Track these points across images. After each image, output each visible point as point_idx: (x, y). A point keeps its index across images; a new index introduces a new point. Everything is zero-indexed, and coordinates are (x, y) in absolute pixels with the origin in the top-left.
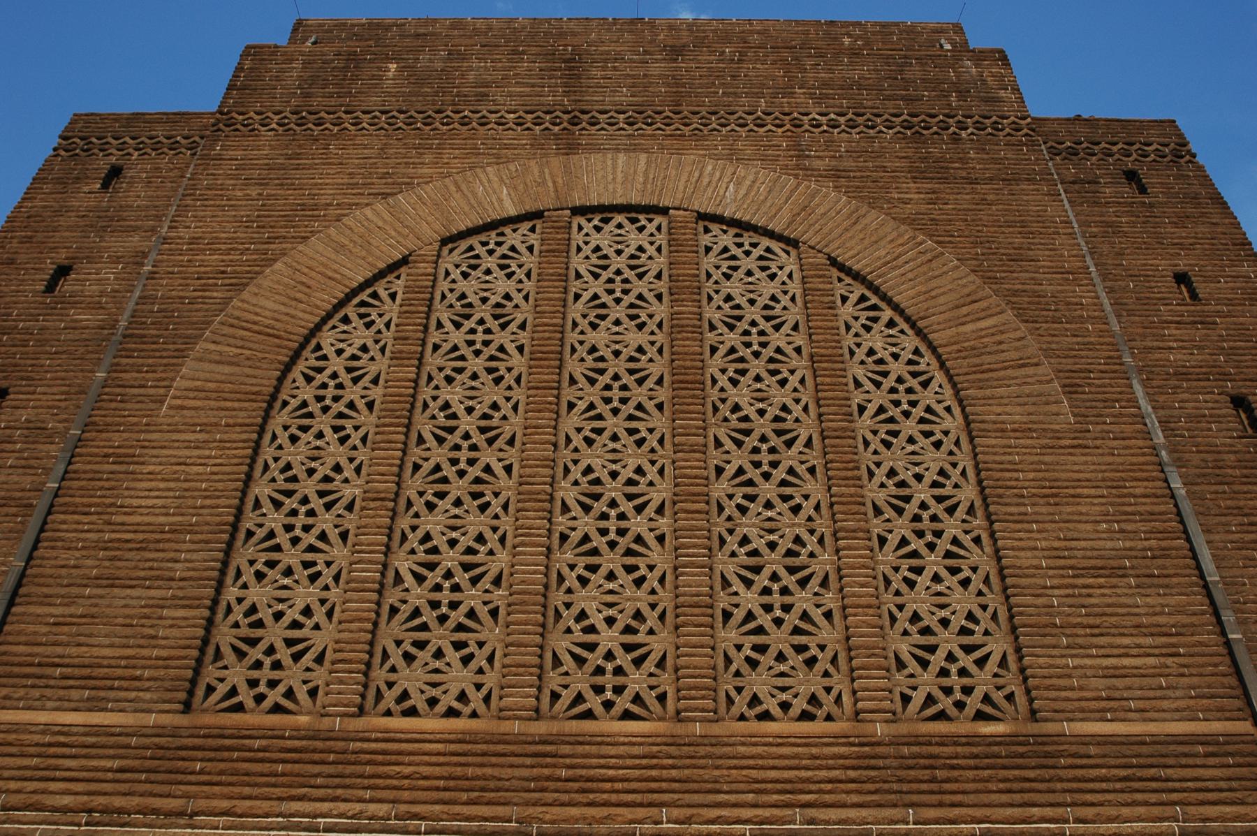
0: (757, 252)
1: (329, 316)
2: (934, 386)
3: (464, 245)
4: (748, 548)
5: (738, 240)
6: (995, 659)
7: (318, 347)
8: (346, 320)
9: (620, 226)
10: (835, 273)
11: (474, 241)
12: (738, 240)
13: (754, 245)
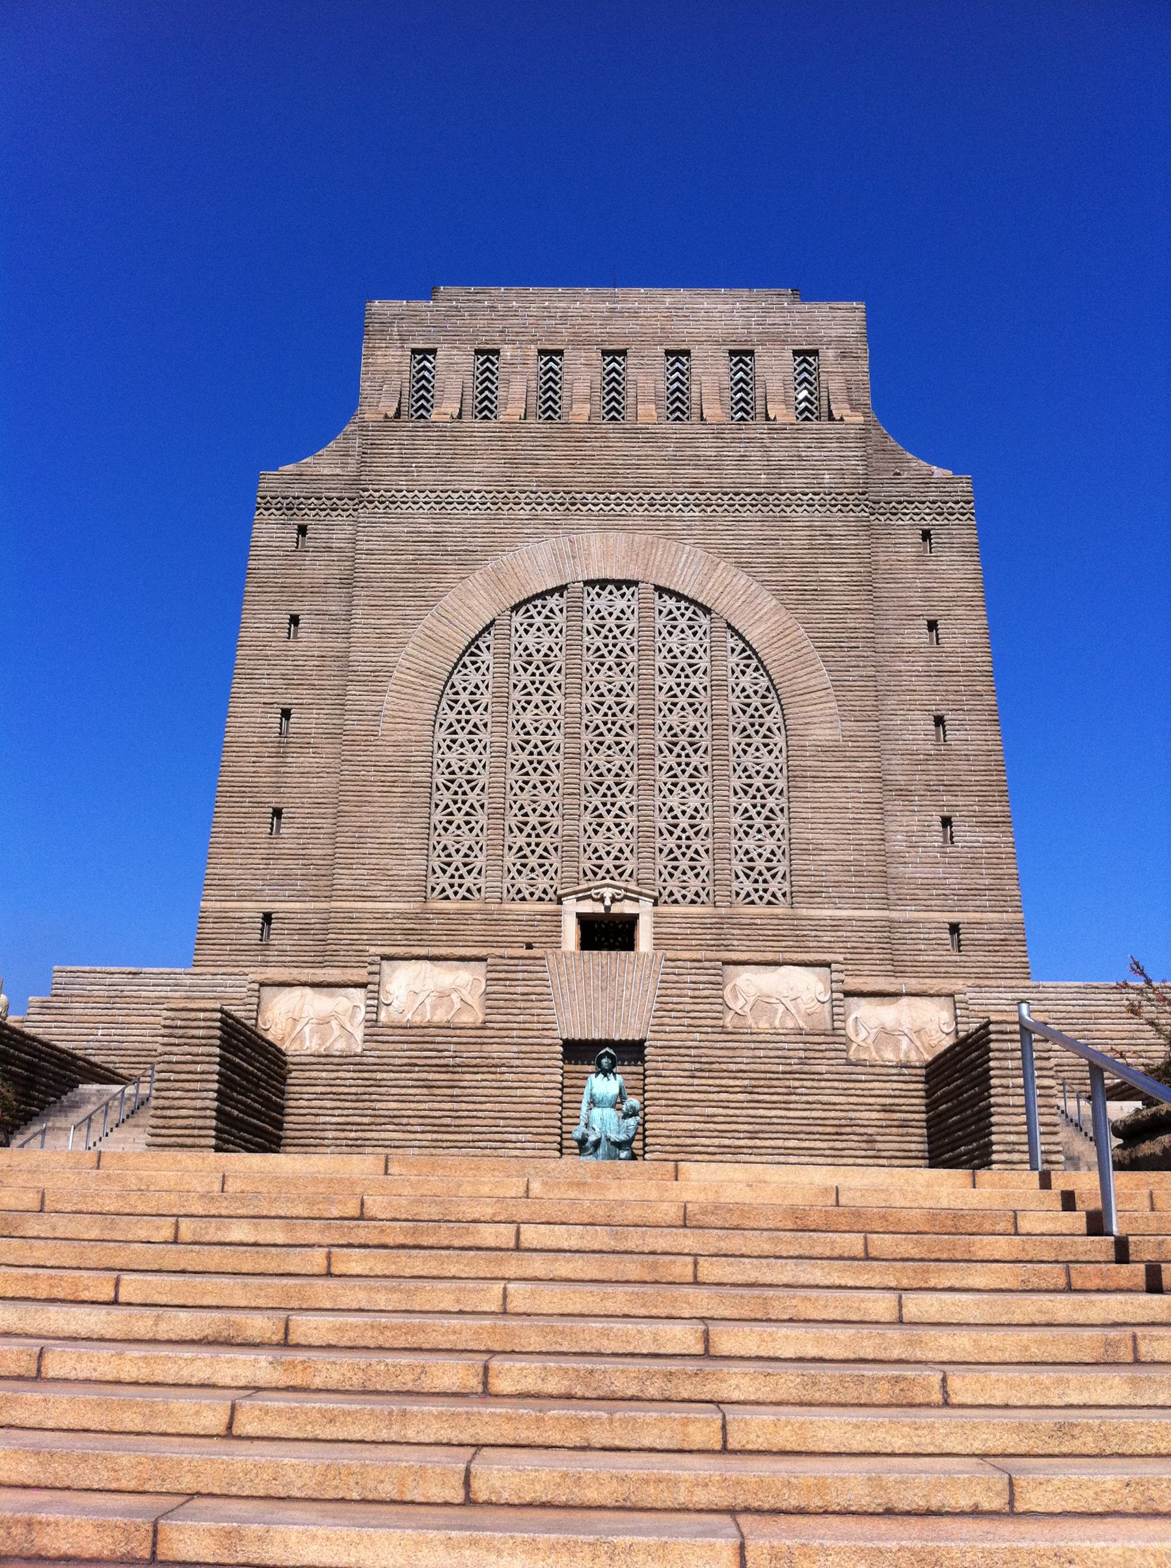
0: (689, 614)
1: (456, 665)
2: (773, 713)
3: (524, 608)
4: (673, 814)
5: (678, 604)
6: (780, 875)
7: (453, 686)
8: (465, 666)
9: (611, 593)
10: (729, 632)
11: (530, 607)
12: (678, 604)
13: (687, 609)
